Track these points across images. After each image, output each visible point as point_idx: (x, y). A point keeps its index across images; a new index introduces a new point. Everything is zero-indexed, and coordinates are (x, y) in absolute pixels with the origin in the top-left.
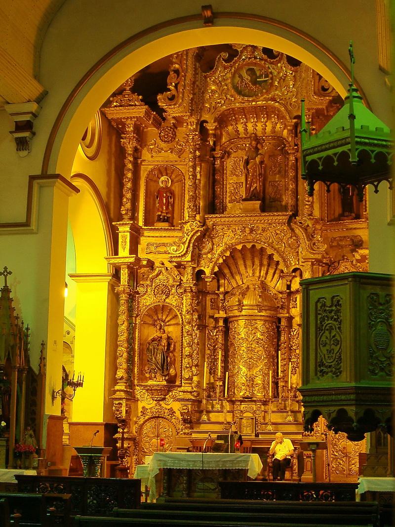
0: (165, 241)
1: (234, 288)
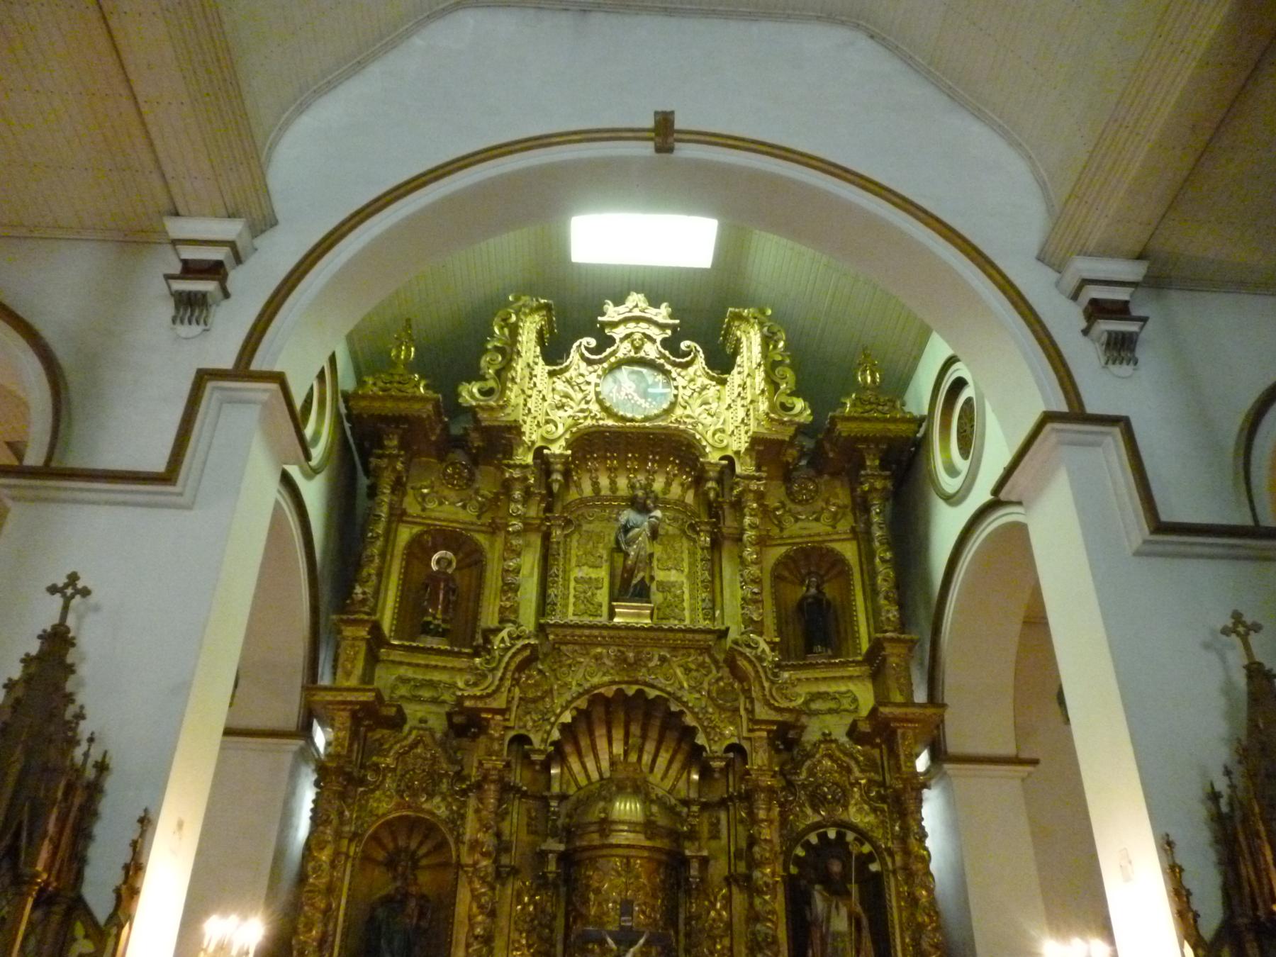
0: (436, 676)
1: (580, 788)
